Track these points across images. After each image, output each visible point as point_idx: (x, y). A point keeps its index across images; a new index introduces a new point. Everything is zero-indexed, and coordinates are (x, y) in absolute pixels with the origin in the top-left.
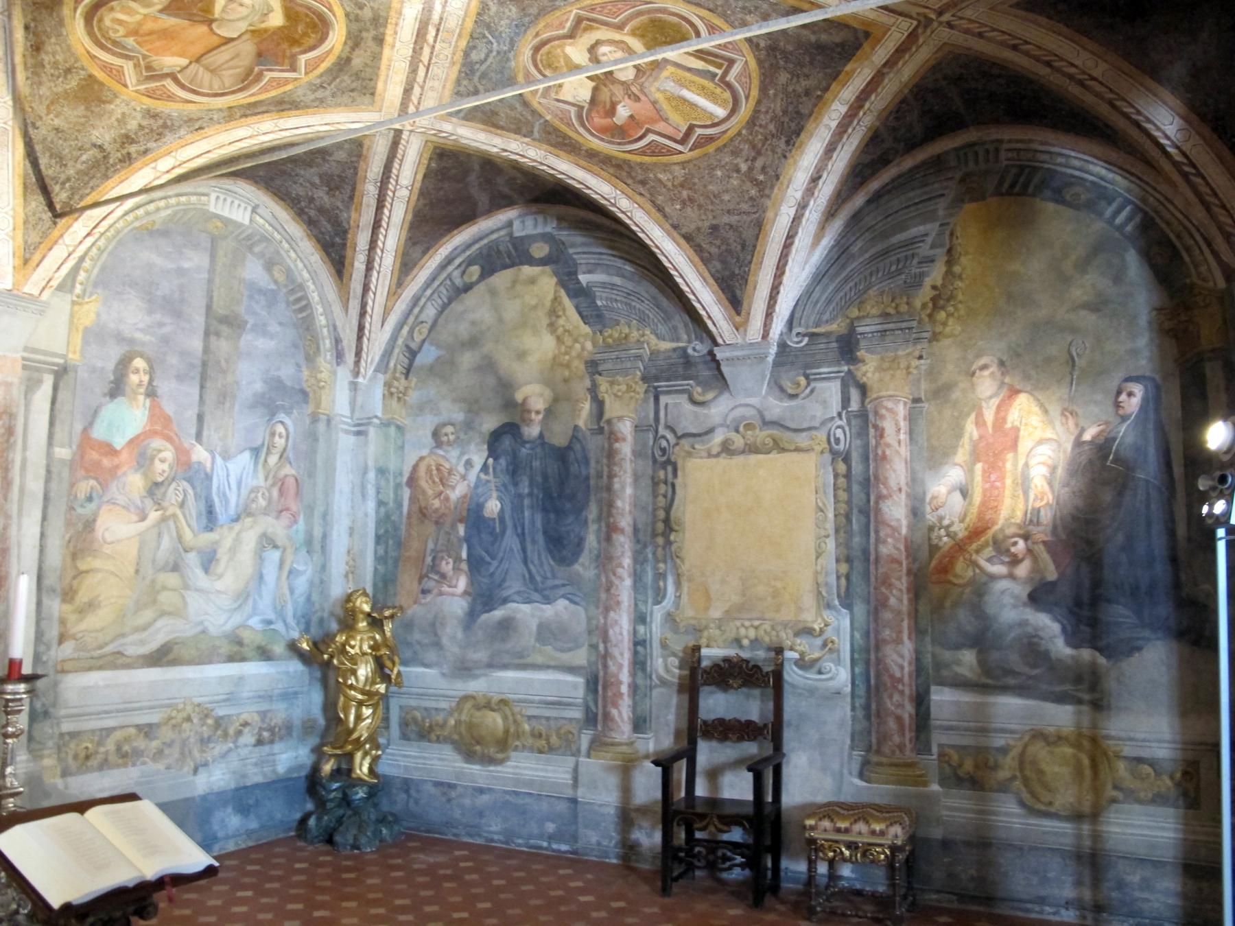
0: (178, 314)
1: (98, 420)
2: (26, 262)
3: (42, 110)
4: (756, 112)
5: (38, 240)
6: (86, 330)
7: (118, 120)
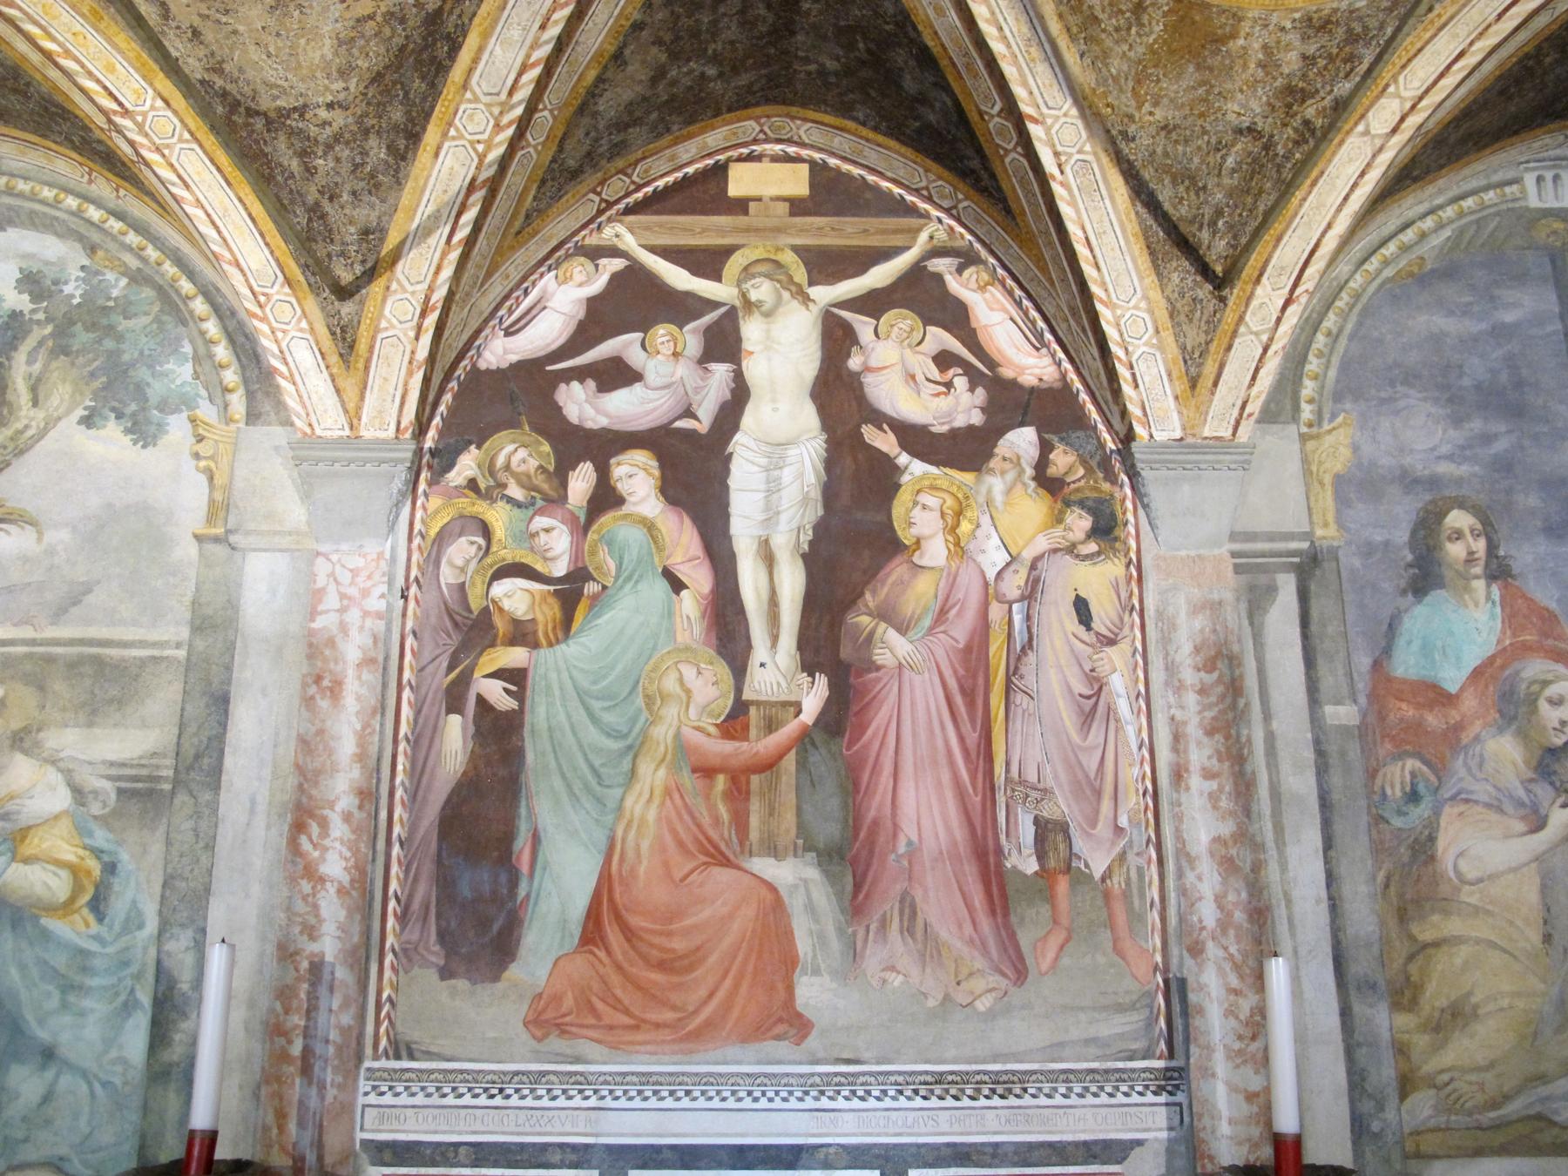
0: (1516, 412)
1: (1401, 642)
2: (1193, 383)
3: (1126, 102)
5: (1202, 338)
6: (1339, 481)
7: (1260, 65)
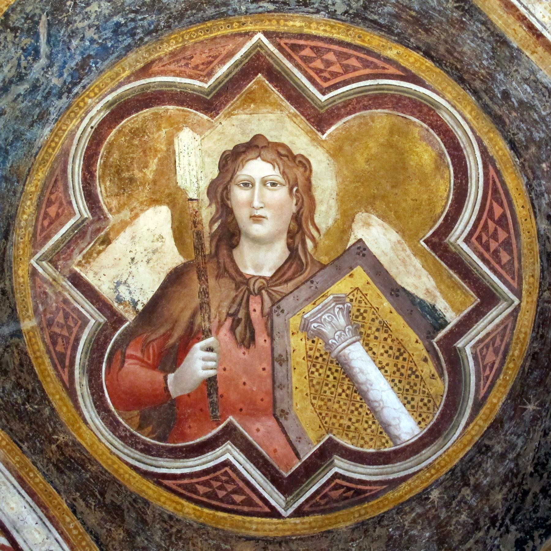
4: (482, 449)
